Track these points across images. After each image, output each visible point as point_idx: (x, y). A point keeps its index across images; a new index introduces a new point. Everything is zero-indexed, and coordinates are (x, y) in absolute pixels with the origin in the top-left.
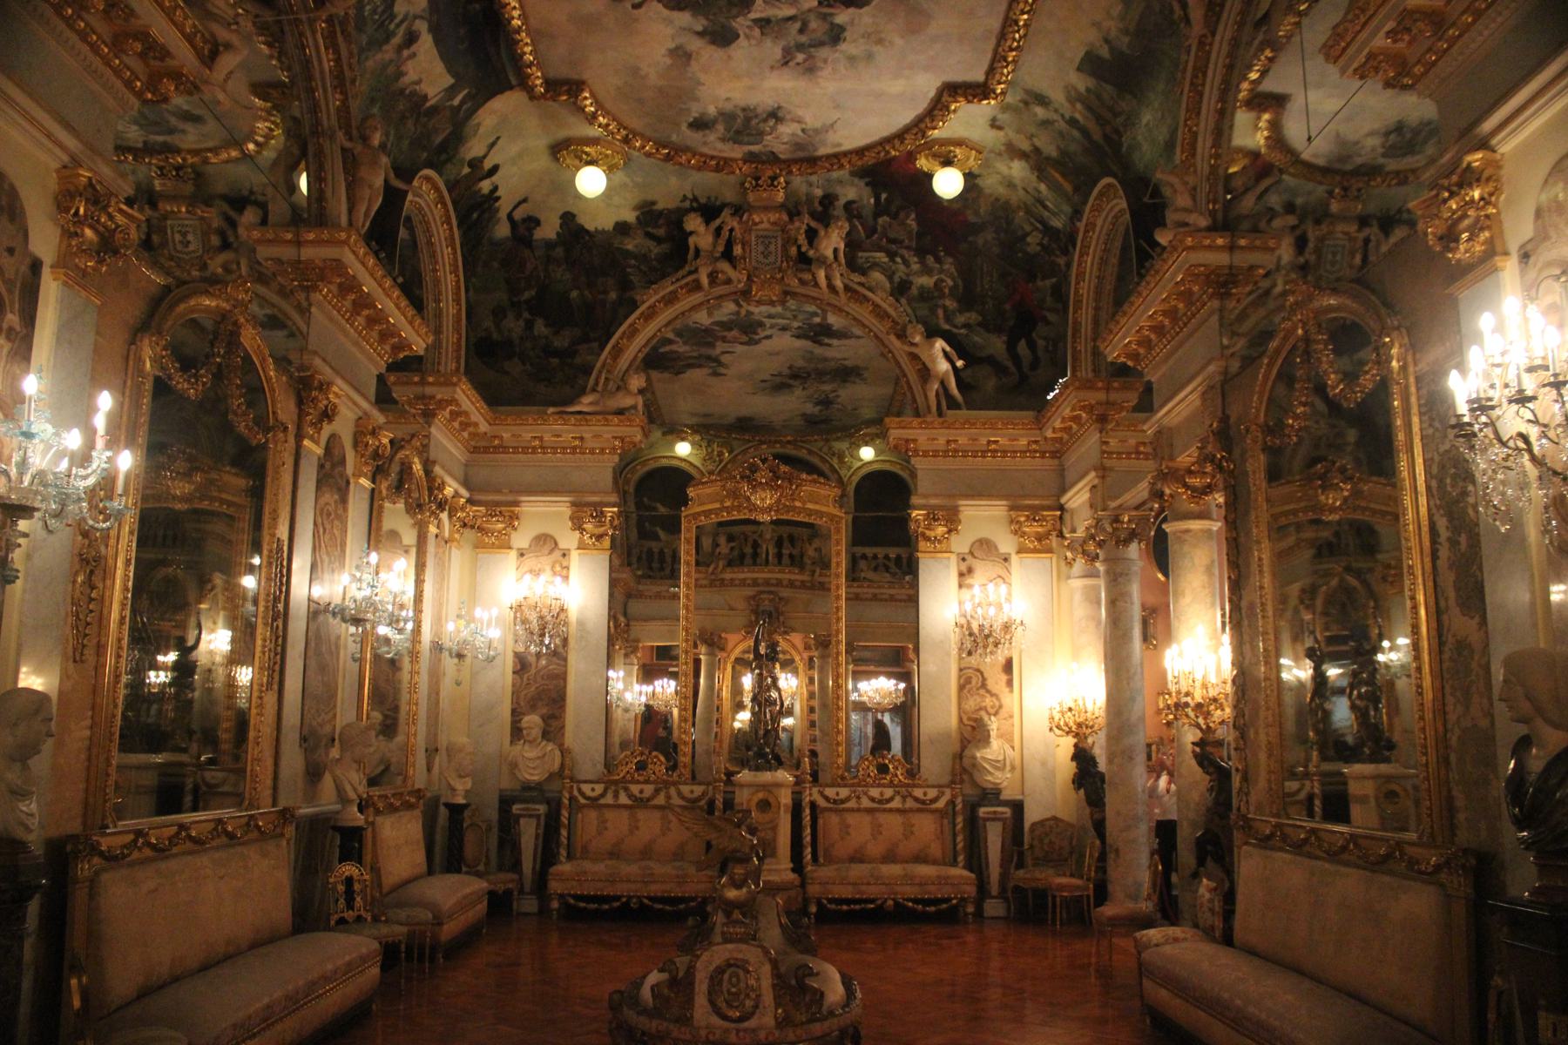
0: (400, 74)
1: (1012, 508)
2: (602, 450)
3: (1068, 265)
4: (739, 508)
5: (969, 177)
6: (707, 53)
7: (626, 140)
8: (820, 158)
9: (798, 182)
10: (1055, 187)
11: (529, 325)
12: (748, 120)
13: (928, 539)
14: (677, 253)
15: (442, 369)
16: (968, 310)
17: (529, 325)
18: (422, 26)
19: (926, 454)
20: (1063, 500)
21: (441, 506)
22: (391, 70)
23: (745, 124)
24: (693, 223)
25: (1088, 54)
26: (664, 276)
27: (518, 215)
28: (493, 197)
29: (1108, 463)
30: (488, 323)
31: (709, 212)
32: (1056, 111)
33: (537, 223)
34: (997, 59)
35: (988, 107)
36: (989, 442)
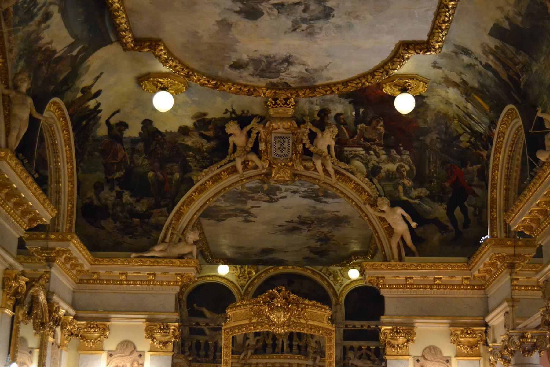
0: (40, 39)
1: (452, 325)
2: (168, 282)
3: (488, 157)
4: (262, 324)
5: (419, 98)
6: (242, 24)
7: (188, 76)
8: (318, 87)
9: (304, 104)
10: (476, 105)
11: (119, 195)
12: (269, 63)
13: (393, 346)
14: (221, 148)
15: (60, 228)
16: (420, 187)
17: (119, 195)
18: (54, 9)
19: (391, 287)
20: (487, 319)
21: (57, 322)
22: (33, 36)
23: (266, 66)
24: (232, 128)
25: (495, 25)
26: (211, 164)
27: (113, 121)
28: (97, 110)
29: (517, 294)
30: (91, 194)
31: (243, 120)
32: (476, 59)
33: (126, 126)
34: (435, 28)
35: (430, 56)
36: (435, 278)
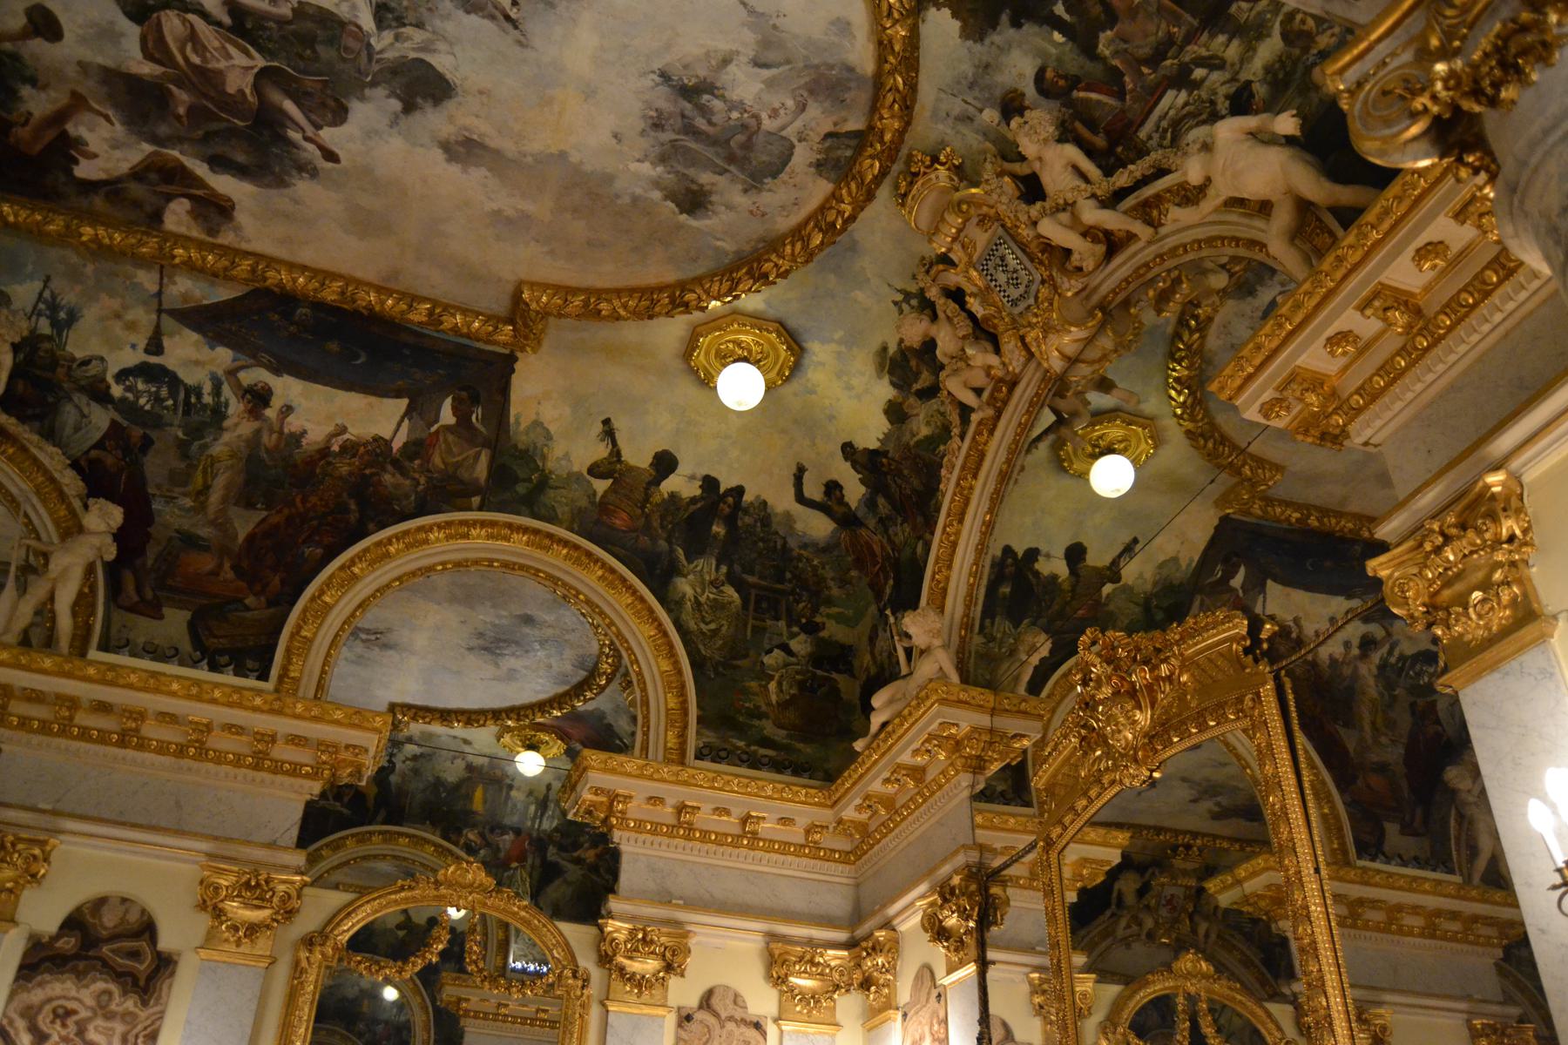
27: (813, 491)
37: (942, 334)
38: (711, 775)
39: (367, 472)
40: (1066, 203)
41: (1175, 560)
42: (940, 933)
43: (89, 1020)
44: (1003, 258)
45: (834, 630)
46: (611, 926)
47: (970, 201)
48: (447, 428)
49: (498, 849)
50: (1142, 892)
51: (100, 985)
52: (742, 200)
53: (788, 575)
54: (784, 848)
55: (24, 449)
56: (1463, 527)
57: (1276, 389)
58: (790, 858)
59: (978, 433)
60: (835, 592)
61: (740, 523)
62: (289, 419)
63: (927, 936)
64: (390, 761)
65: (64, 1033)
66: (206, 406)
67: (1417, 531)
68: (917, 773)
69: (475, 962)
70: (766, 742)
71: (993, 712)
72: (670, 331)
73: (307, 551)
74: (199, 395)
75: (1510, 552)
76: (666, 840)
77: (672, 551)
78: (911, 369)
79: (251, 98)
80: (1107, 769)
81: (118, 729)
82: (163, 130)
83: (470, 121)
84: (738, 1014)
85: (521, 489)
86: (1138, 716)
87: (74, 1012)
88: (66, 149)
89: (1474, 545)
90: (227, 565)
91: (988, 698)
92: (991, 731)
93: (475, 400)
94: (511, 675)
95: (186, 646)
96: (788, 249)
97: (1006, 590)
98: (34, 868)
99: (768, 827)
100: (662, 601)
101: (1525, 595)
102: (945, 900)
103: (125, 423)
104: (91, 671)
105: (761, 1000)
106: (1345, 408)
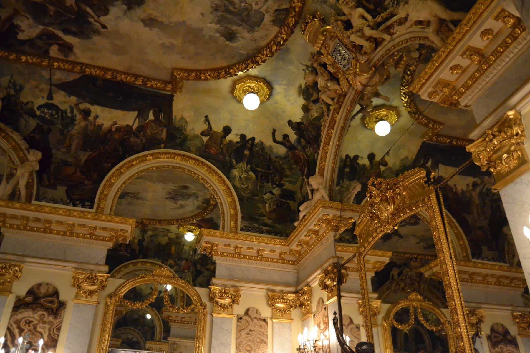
18: (85, 106)
27: (279, 138)
37: (320, 80)
38: (246, 236)
39: (125, 137)
40: (360, 29)
41: (407, 158)
42: (325, 287)
43: (37, 324)
44: (339, 51)
45: (288, 186)
46: (213, 288)
47: (326, 30)
48: (151, 121)
49: (181, 266)
50: (400, 274)
51: (40, 313)
52: (247, 35)
53: (272, 168)
54: (272, 260)
55: (7, 134)
56: (500, 131)
57: (433, 87)
58: (274, 264)
59: (334, 114)
60: (288, 173)
61: (254, 150)
62: (98, 120)
63: (321, 288)
64: (143, 238)
65: (29, 328)
66: (68, 117)
67: (484, 135)
68: (316, 232)
69: (167, 301)
70: (265, 225)
71: (341, 210)
72: (226, 83)
73: (105, 165)
74: (66, 113)
75: (517, 139)
76: (231, 259)
77: (231, 160)
78: (309, 92)
79: (76, 8)
80: (379, 227)
81: (43, 227)
82: (46, 21)
83: (150, 12)
84: (258, 317)
85: (178, 141)
86: (389, 207)
87: (32, 322)
88: (15, 29)
89: (504, 138)
90: (78, 171)
91: (339, 205)
92: (341, 217)
93: (160, 111)
94: (182, 206)
95: (65, 198)
96: (265, 52)
97: (347, 170)
98: (17, 274)
99: (266, 253)
100: (228, 178)
101: (523, 155)
102: (326, 275)
103: (41, 124)
104: (32, 207)
105: (266, 312)
106: (458, 93)
